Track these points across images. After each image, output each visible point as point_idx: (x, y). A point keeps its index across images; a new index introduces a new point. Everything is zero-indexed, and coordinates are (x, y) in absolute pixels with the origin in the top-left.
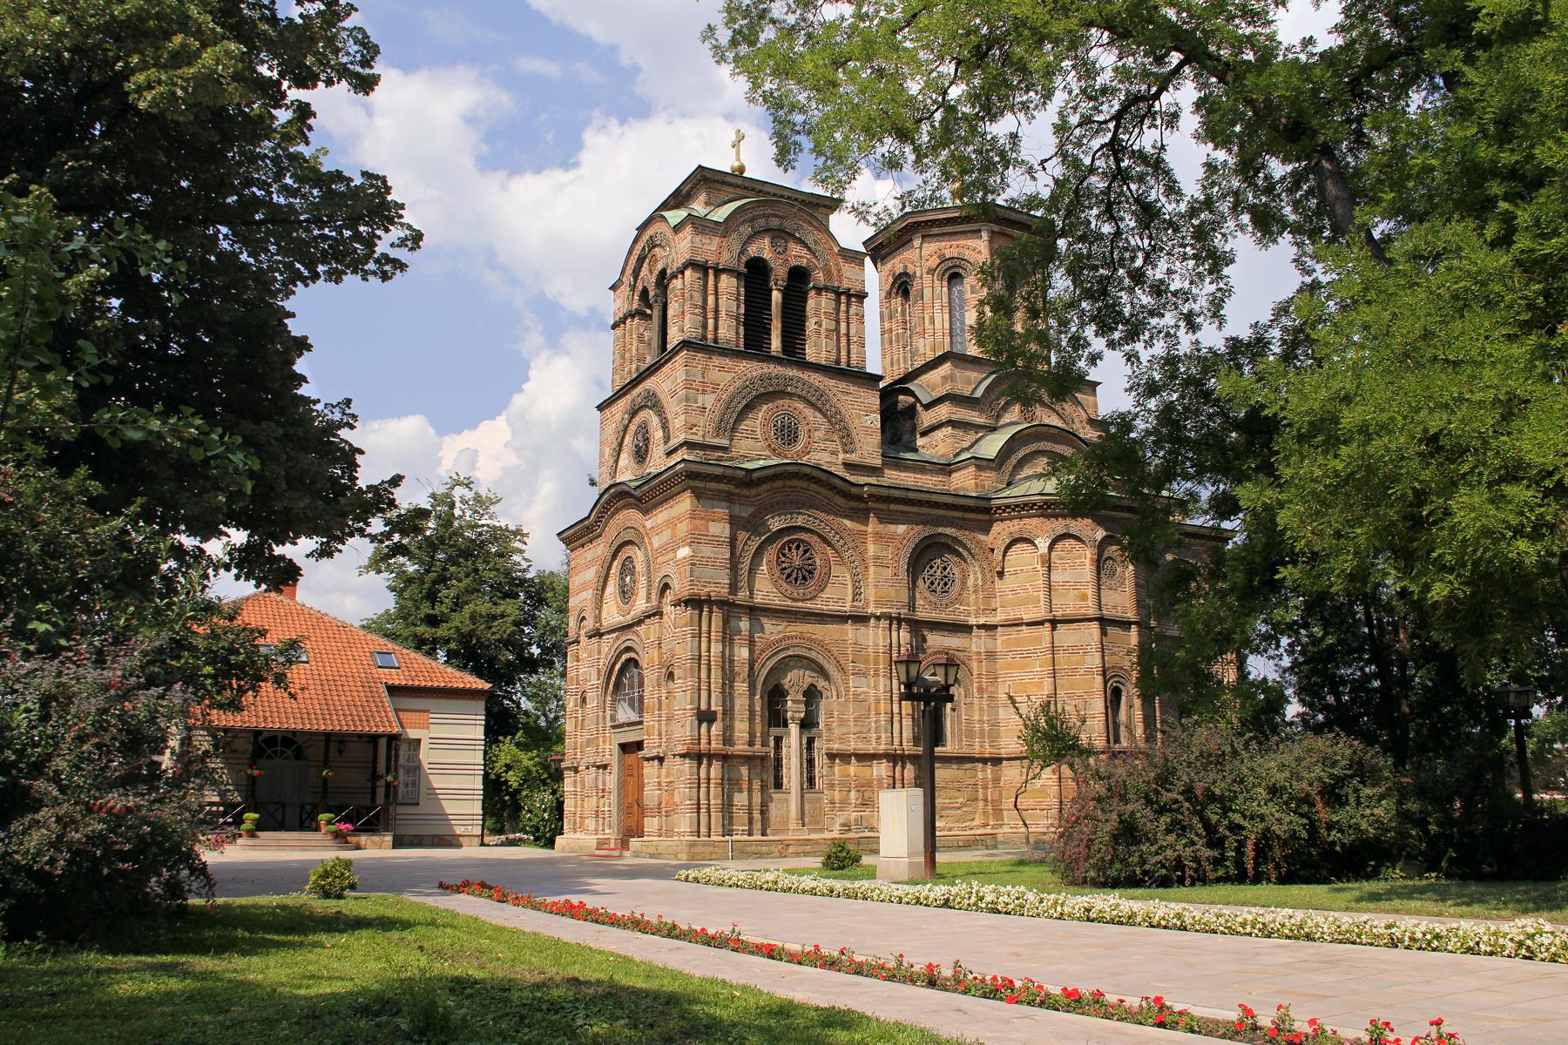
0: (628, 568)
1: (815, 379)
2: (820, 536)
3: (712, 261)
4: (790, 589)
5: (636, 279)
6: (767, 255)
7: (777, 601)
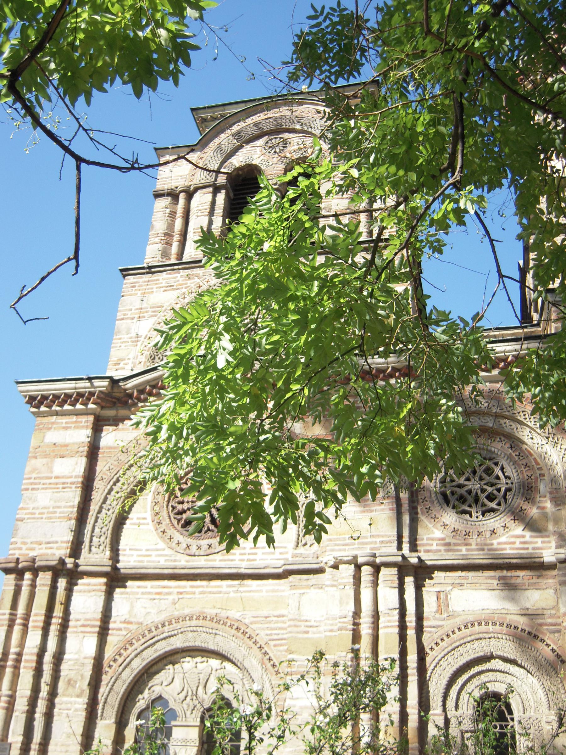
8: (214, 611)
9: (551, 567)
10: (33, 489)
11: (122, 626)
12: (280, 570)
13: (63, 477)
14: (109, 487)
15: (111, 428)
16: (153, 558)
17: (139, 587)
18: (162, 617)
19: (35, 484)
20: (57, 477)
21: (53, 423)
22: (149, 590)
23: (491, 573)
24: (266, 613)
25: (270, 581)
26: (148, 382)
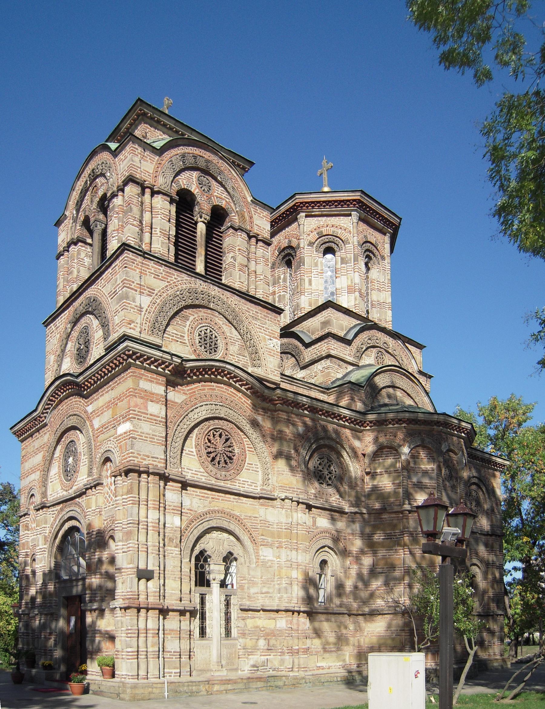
0: (71, 450)
1: (233, 300)
4: (214, 470)
7: (203, 478)
8: (228, 510)
9: (346, 513)
10: (138, 419)
11: (188, 511)
12: (258, 496)
13: (154, 416)
14: (175, 428)
15: (172, 388)
16: (199, 477)
17: (193, 491)
18: (206, 509)
19: (139, 416)
20: (151, 415)
21: (143, 375)
22: (198, 494)
23: (328, 512)
24: (249, 515)
25: (251, 499)
26: (196, 366)
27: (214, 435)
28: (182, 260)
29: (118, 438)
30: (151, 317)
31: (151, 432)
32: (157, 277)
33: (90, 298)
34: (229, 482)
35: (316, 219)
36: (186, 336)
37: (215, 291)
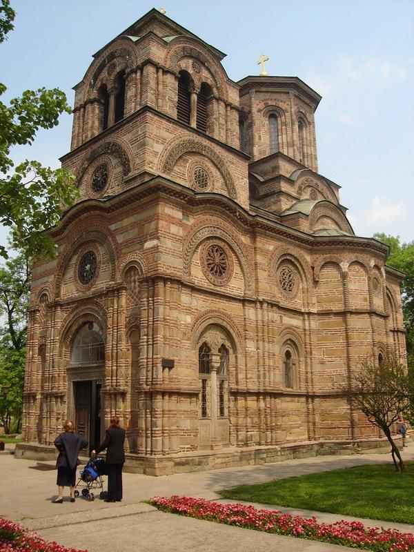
1: (218, 150)
2: (229, 245)
3: (162, 63)
4: (213, 278)
5: (95, 81)
6: (191, 71)
7: (206, 285)
13: (175, 235)
27: (217, 251)
28: (183, 118)
29: (145, 252)
30: (164, 159)
31: (172, 247)
32: (167, 130)
33: (109, 143)
34: (223, 288)
35: (262, 94)
36: (186, 174)
37: (206, 142)
